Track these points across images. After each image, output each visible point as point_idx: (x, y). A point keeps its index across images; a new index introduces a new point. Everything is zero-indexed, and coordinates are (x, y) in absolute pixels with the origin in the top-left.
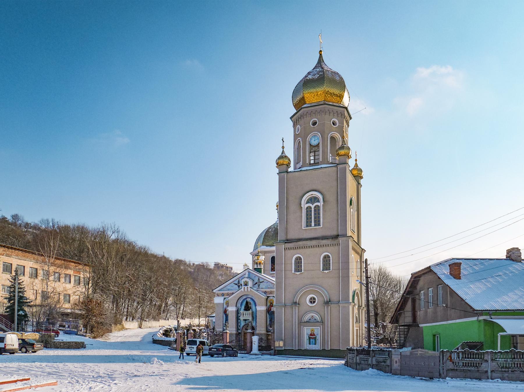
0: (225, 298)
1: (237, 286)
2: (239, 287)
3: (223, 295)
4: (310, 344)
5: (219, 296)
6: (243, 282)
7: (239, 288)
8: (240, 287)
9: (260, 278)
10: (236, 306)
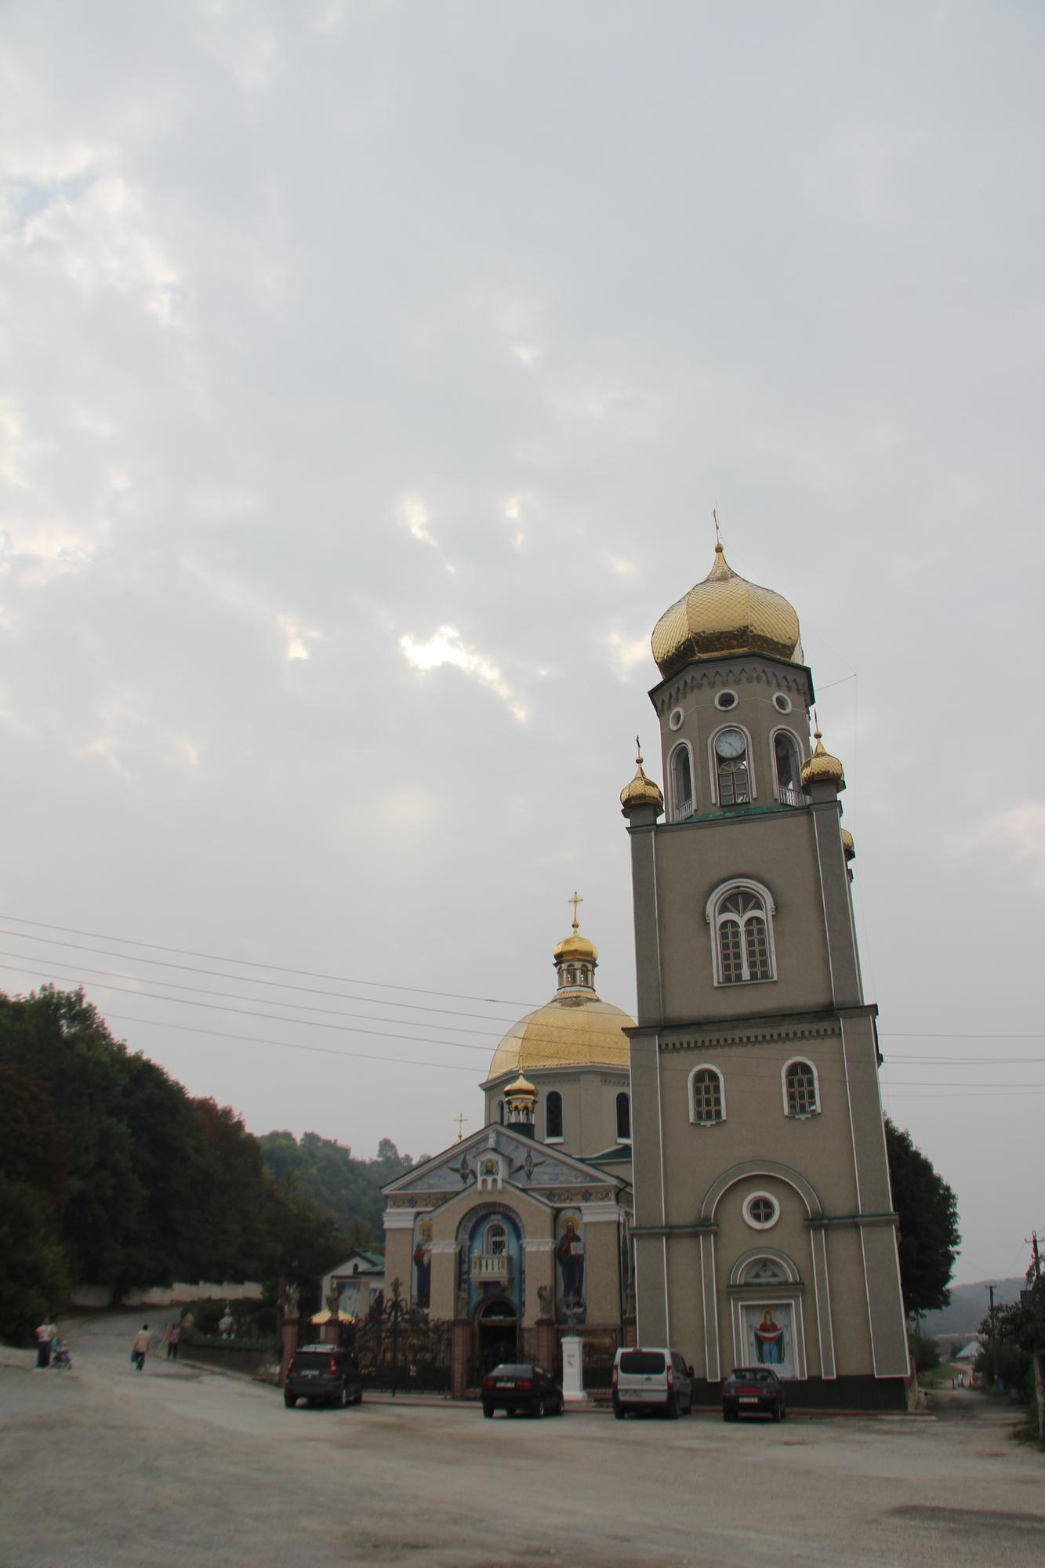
1: (458, 1176)
2: (464, 1177)
3: (412, 1201)
4: (761, 1359)
6: (482, 1163)
7: (465, 1182)
8: (470, 1180)
10: (456, 1239)
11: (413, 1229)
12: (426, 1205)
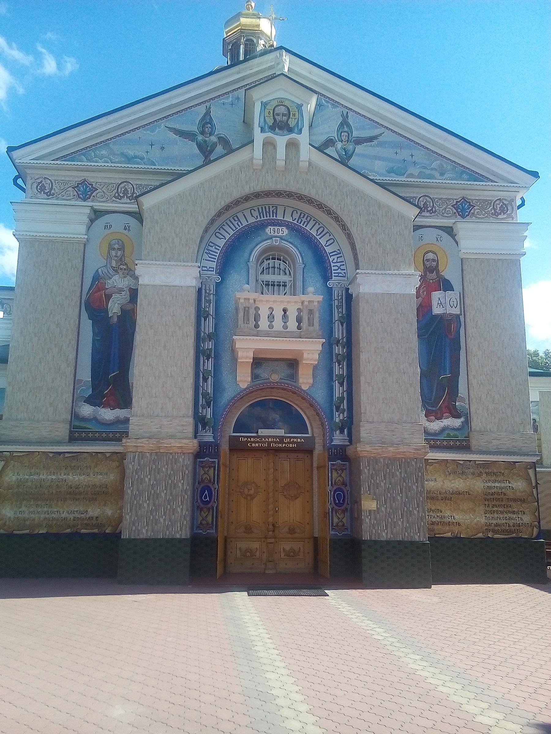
0: (97, 214)
5: (49, 194)
6: (264, 105)
9: (350, 114)
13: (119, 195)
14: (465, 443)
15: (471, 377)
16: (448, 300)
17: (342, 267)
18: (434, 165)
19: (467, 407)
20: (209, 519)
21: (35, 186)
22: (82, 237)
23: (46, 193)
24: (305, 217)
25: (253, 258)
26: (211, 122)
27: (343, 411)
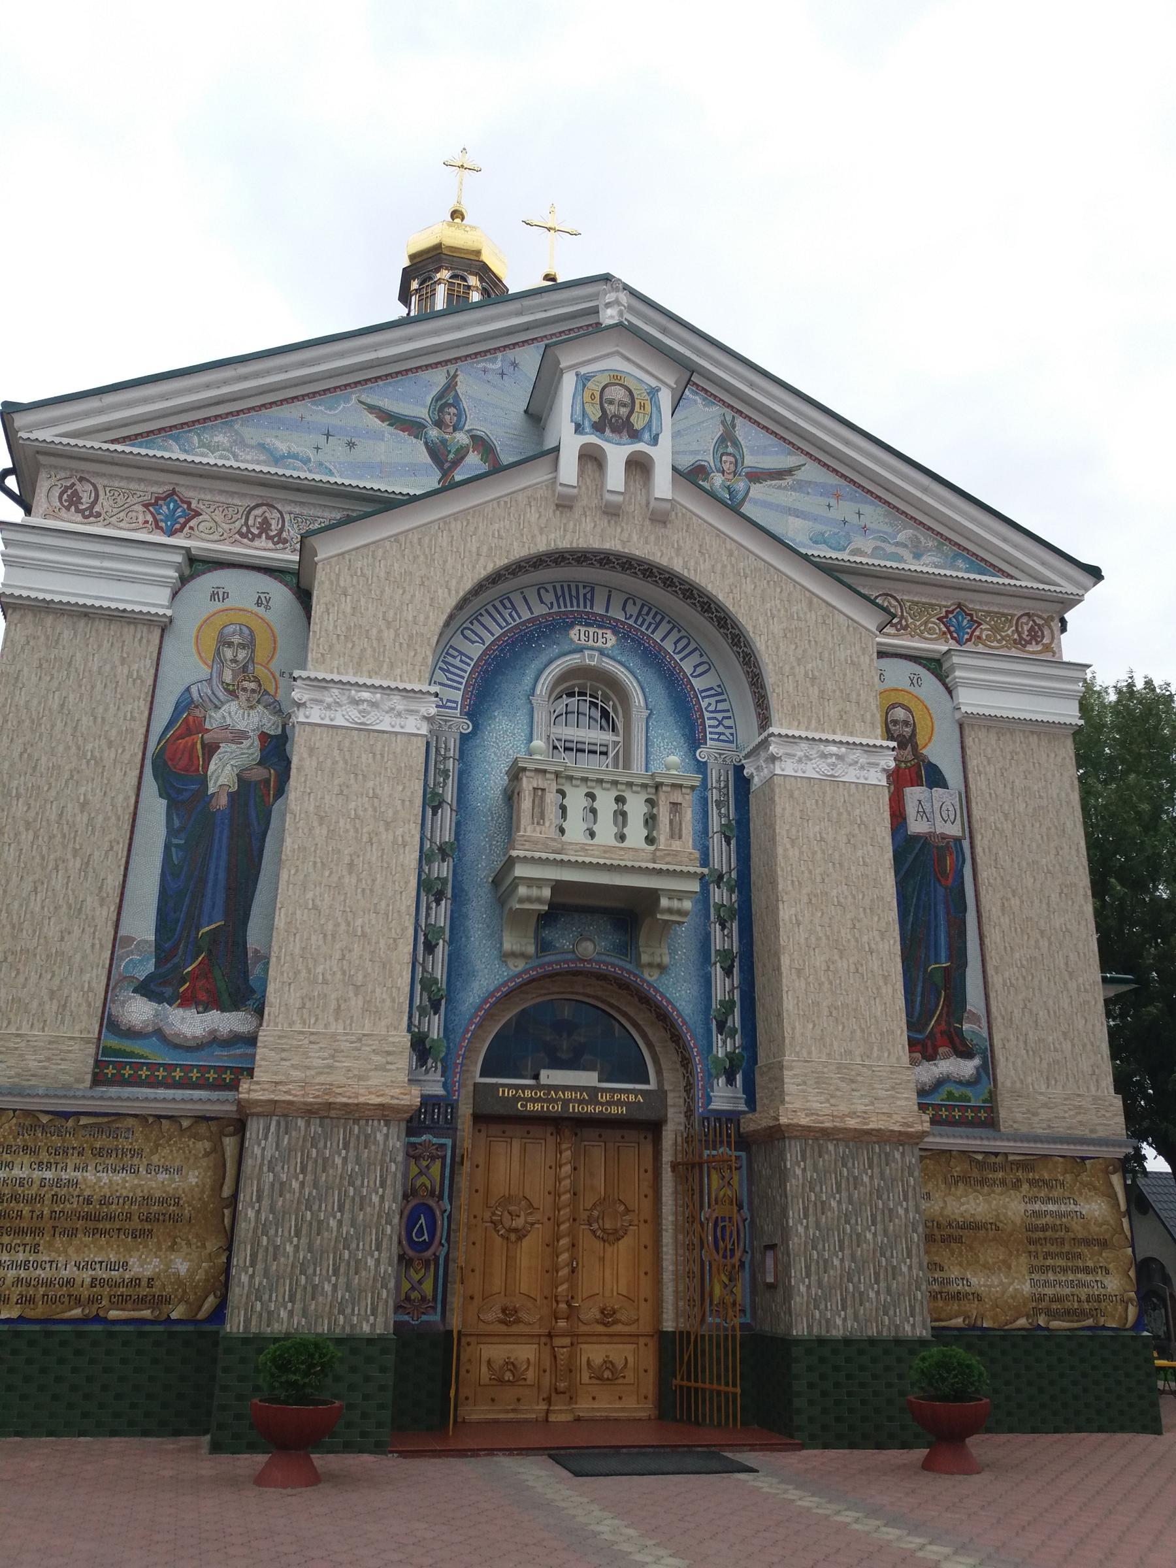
6: (584, 380)
11: (164, 626)
12: (246, 535)
13: (249, 531)
14: (983, 1115)
15: (991, 971)
16: (937, 806)
17: (727, 722)
18: (901, 537)
19: (985, 1035)
20: (427, 1287)
21: (56, 492)
22: (161, 612)
23: (82, 512)
24: (651, 615)
25: (542, 688)
26: (456, 403)
27: (734, 1031)
